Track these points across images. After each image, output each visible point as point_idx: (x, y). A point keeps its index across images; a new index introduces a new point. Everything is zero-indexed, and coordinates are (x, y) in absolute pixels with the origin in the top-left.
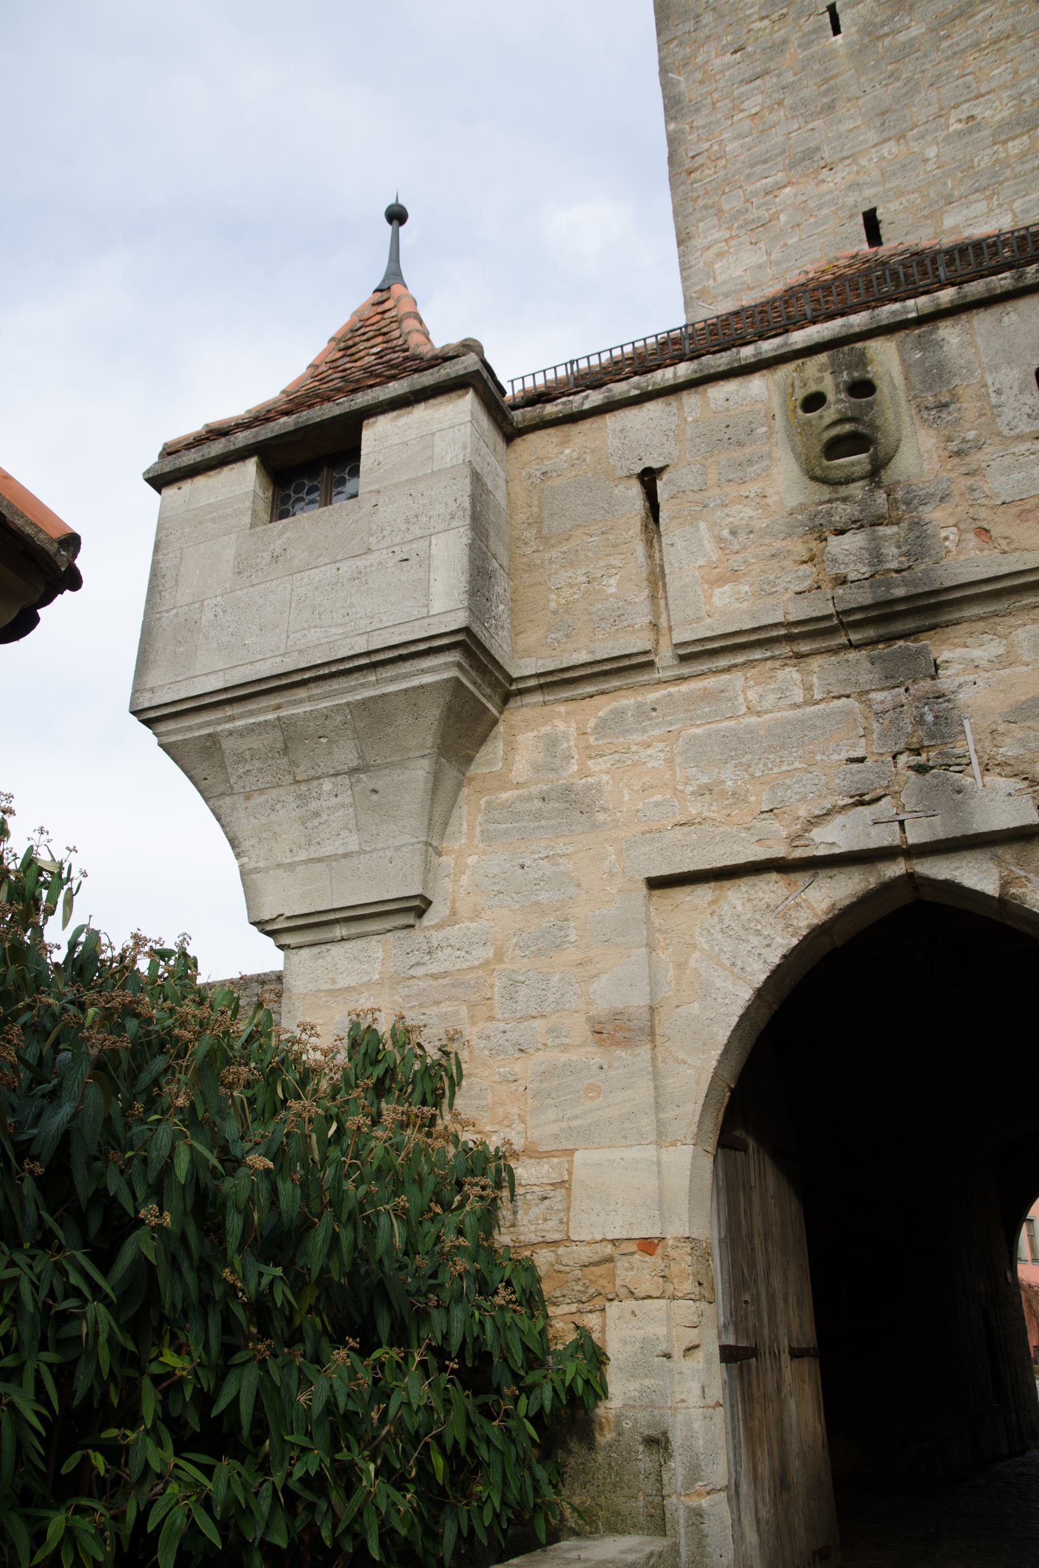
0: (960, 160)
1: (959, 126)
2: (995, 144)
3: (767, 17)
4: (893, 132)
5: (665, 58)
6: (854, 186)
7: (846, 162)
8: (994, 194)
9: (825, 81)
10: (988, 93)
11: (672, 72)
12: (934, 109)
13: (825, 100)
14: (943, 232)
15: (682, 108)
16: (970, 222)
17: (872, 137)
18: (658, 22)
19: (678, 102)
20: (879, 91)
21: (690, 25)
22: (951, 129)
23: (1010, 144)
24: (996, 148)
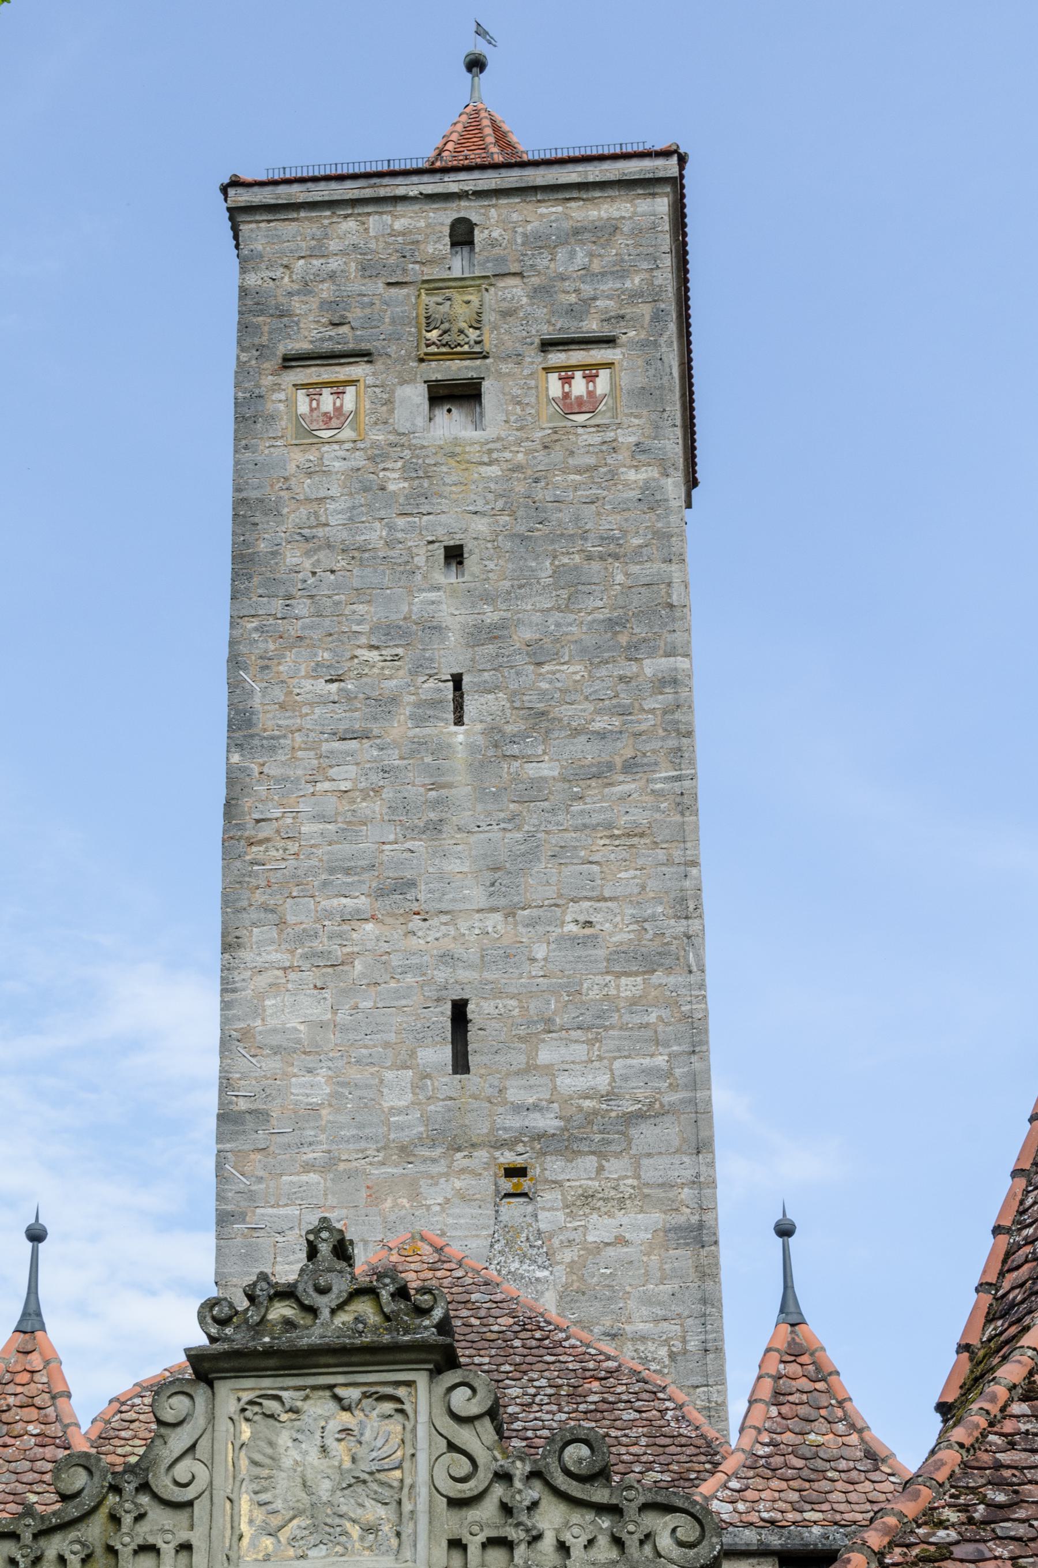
0: (568, 977)
1: (573, 928)
2: (607, 973)
3: (377, 648)
4: (502, 902)
5: (239, 642)
6: (447, 958)
7: (445, 918)
8: (596, 1039)
9: (436, 786)
10: (611, 899)
11: (244, 670)
12: (551, 892)
13: (432, 815)
14: (536, 1067)
15: (252, 736)
16: (566, 1067)
17: (477, 896)
18: (236, 576)
19: (249, 723)
20: (496, 835)
21: (277, 605)
22: (566, 929)
23: (624, 980)
24: (608, 978)
